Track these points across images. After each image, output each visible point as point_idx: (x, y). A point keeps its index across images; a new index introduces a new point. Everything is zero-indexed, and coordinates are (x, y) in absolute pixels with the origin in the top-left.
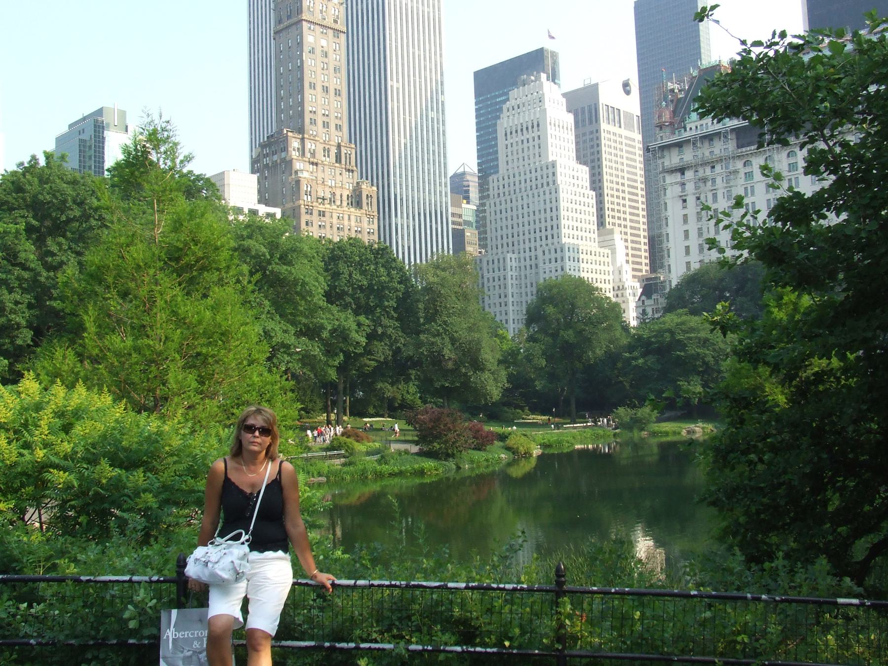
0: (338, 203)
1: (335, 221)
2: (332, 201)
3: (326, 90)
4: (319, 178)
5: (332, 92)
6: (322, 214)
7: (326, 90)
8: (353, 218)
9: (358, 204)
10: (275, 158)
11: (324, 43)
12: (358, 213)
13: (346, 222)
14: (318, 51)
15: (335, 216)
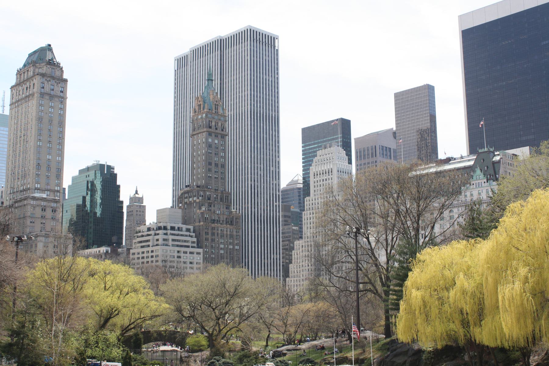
0: (221, 222)
1: (219, 232)
2: (218, 221)
3: (216, 165)
4: (212, 210)
5: (220, 166)
6: (213, 228)
7: (216, 165)
8: (228, 230)
9: (231, 224)
10: (191, 199)
11: (216, 142)
12: (231, 227)
13: (225, 232)
14: (213, 146)
15: (220, 229)
